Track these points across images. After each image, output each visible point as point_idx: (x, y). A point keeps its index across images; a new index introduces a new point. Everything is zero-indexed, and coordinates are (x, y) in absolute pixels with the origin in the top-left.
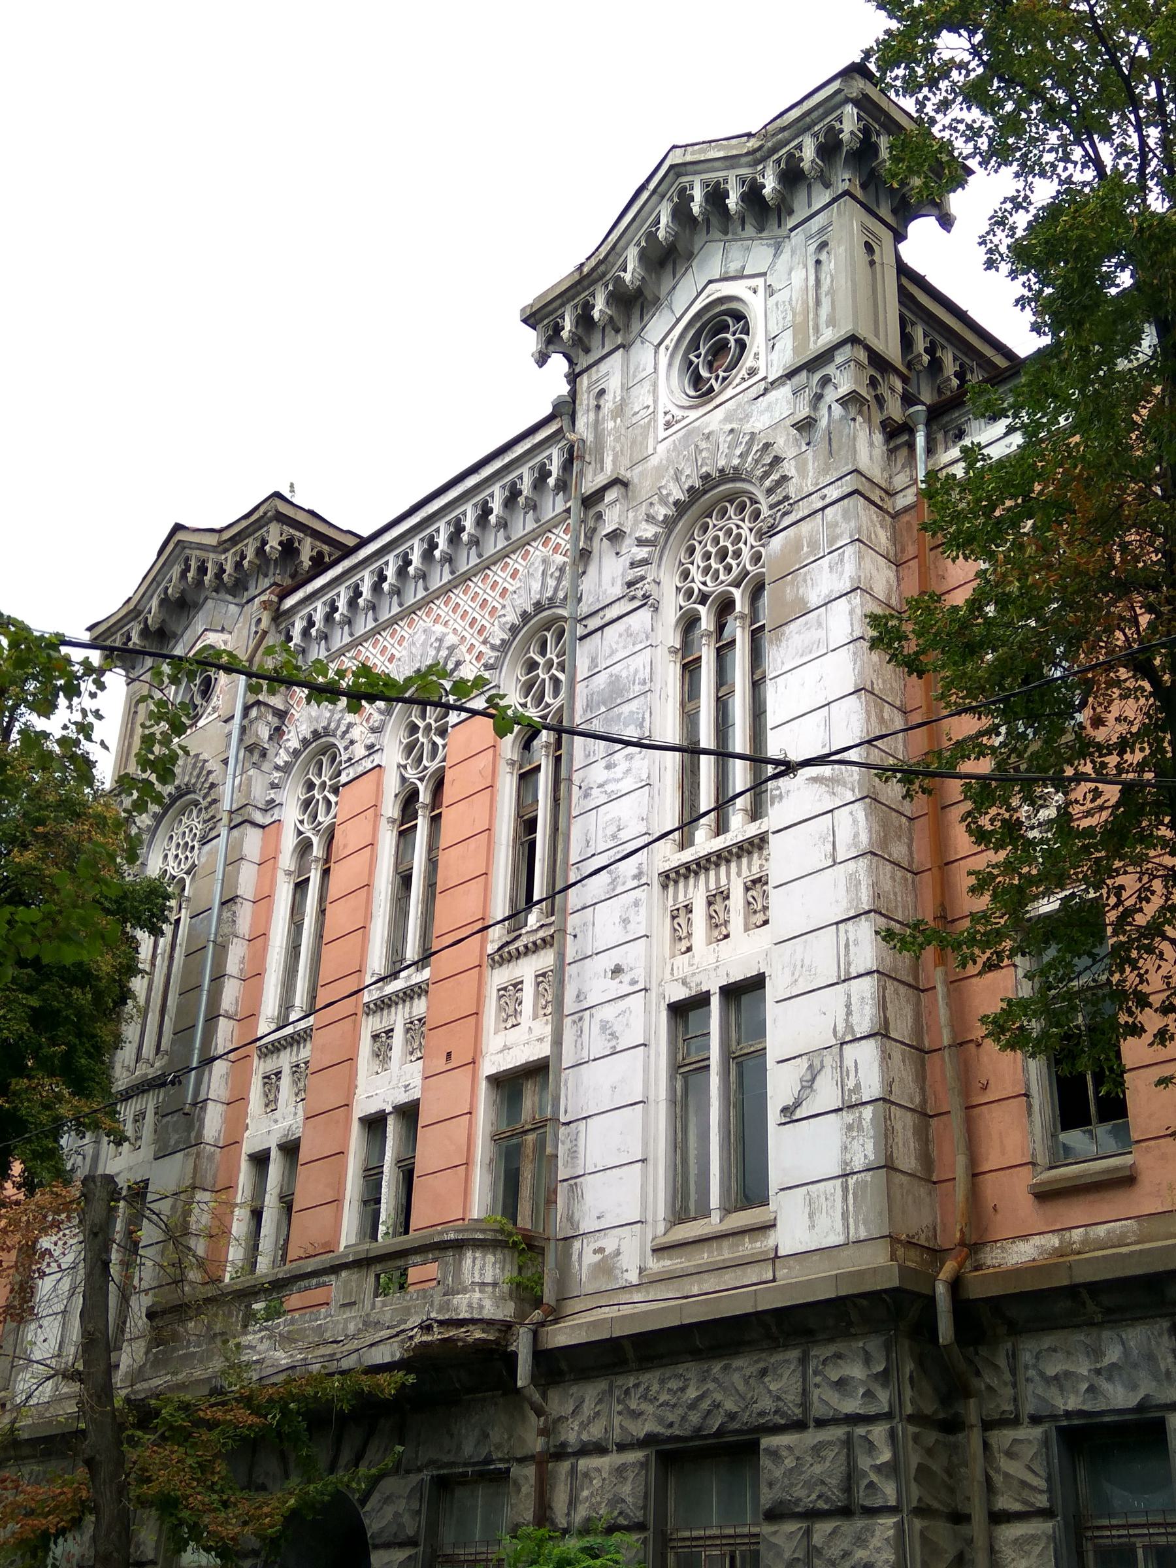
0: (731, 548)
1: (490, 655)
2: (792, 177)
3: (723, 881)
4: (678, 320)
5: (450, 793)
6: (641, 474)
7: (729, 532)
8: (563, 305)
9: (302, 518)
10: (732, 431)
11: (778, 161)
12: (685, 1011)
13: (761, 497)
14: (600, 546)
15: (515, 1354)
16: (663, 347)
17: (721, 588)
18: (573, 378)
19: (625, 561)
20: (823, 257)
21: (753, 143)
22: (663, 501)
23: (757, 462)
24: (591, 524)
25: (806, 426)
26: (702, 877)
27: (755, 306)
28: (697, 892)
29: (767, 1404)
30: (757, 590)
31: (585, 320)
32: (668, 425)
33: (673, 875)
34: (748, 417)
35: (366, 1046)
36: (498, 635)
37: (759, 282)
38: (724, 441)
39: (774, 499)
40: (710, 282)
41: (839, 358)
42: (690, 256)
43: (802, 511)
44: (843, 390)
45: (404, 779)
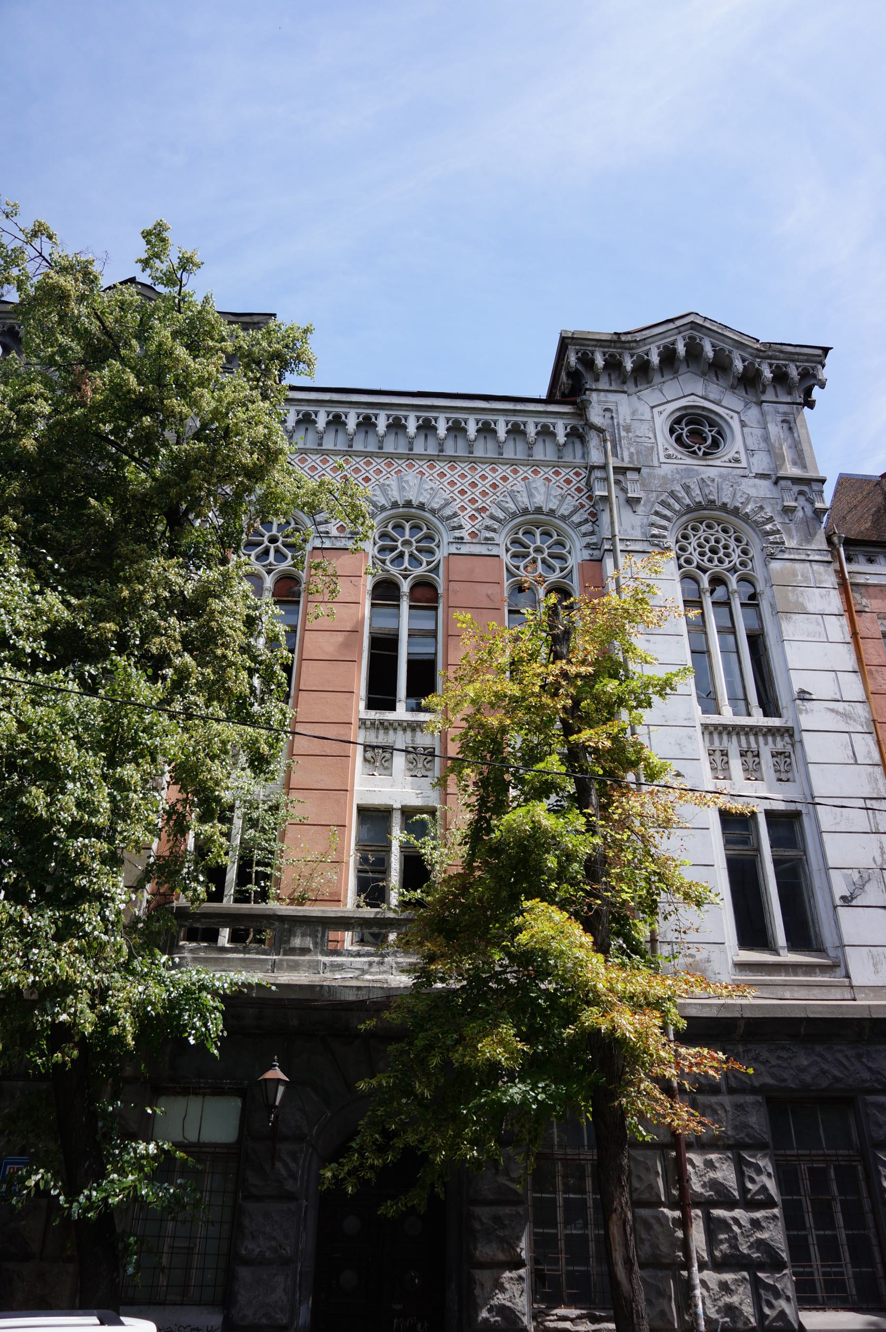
3: (753, 745)
4: (668, 402)
6: (649, 474)
8: (595, 346)
16: (656, 410)
17: (717, 569)
21: (757, 346)
22: (678, 500)
26: (734, 738)
28: (733, 747)
29: (866, 1075)
37: (735, 415)
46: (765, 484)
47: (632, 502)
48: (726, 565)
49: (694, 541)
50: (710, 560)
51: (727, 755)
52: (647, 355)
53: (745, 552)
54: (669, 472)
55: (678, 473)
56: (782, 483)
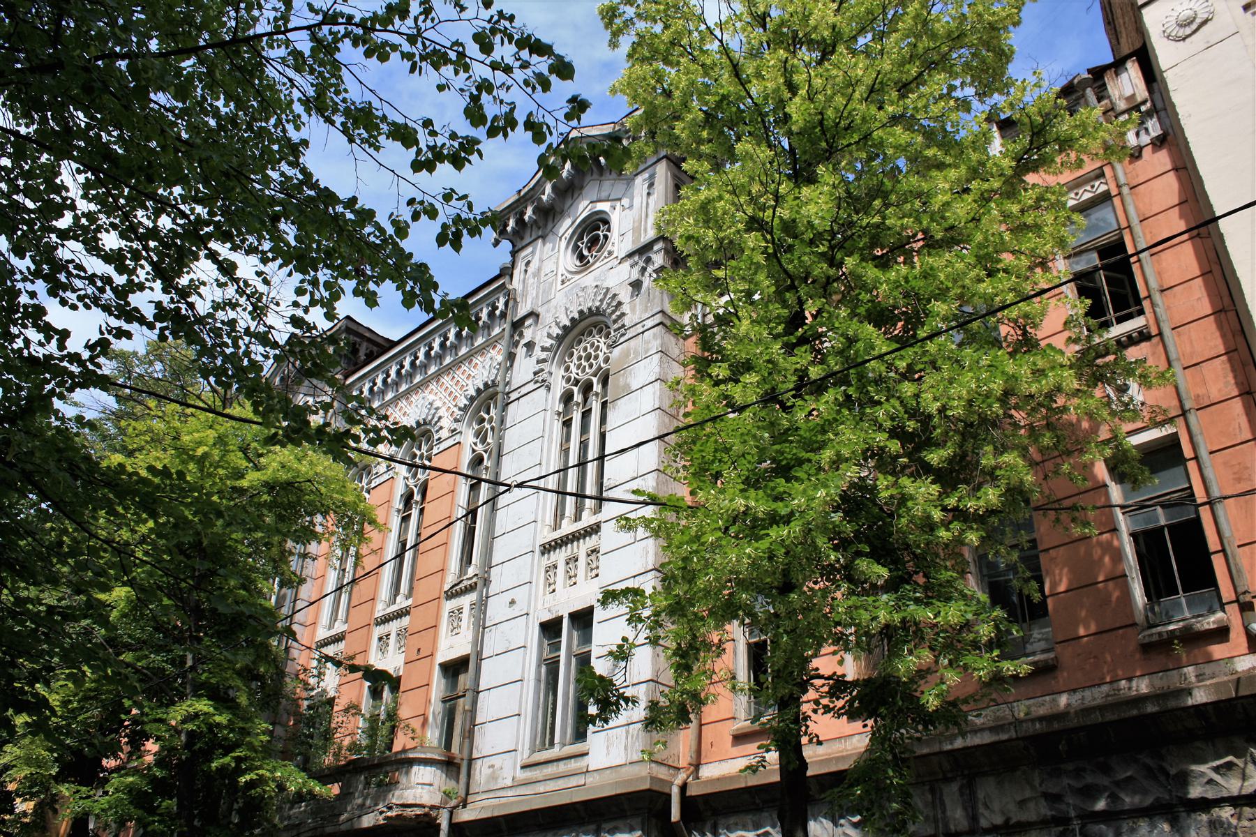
1: (458, 413)
3: (575, 550)
5: (430, 495)
9: (361, 330)
12: (550, 629)
13: (610, 324)
14: (521, 351)
15: (439, 825)
18: (514, 254)
19: (534, 359)
23: (609, 304)
24: (517, 338)
25: (636, 285)
27: (615, 218)
28: (560, 556)
30: (605, 382)
31: (520, 221)
32: (563, 283)
35: (375, 642)
36: (463, 402)
37: (618, 204)
38: (591, 291)
39: (616, 326)
41: (656, 248)
42: (582, 188)
43: (630, 334)
44: (657, 266)
45: (407, 486)
47: (530, 346)
49: (575, 357)
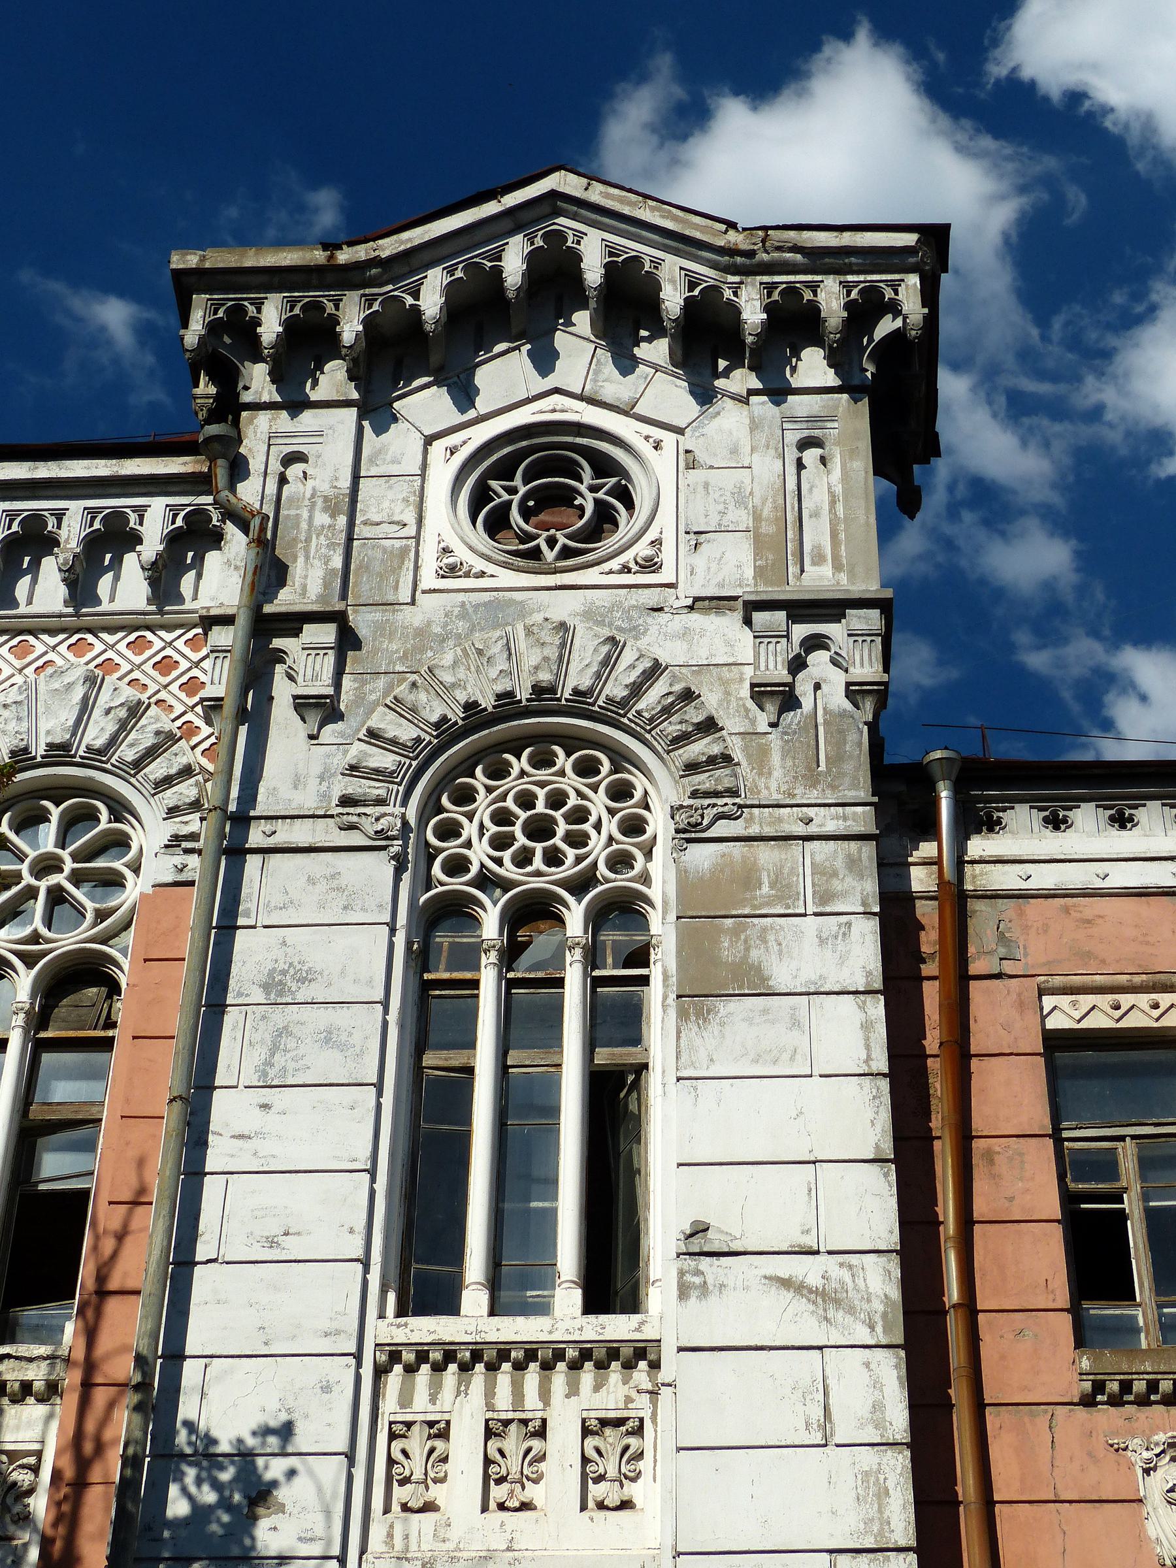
0: (562, 828)
2: (793, 323)
7: (557, 800)
10: (612, 640)
11: (770, 288)
16: (438, 447)
20: (811, 456)
21: (734, 238)
23: (667, 711)
28: (466, 1405)
33: (408, 1356)
34: (637, 632)
37: (668, 438)
40: (557, 391)
46: (730, 623)
48: (567, 870)
49: (483, 805)
50: (524, 858)
51: (444, 1435)
52: (416, 295)
53: (633, 827)
54: (439, 617)
55: (464, 615)
56: (759, 617)
